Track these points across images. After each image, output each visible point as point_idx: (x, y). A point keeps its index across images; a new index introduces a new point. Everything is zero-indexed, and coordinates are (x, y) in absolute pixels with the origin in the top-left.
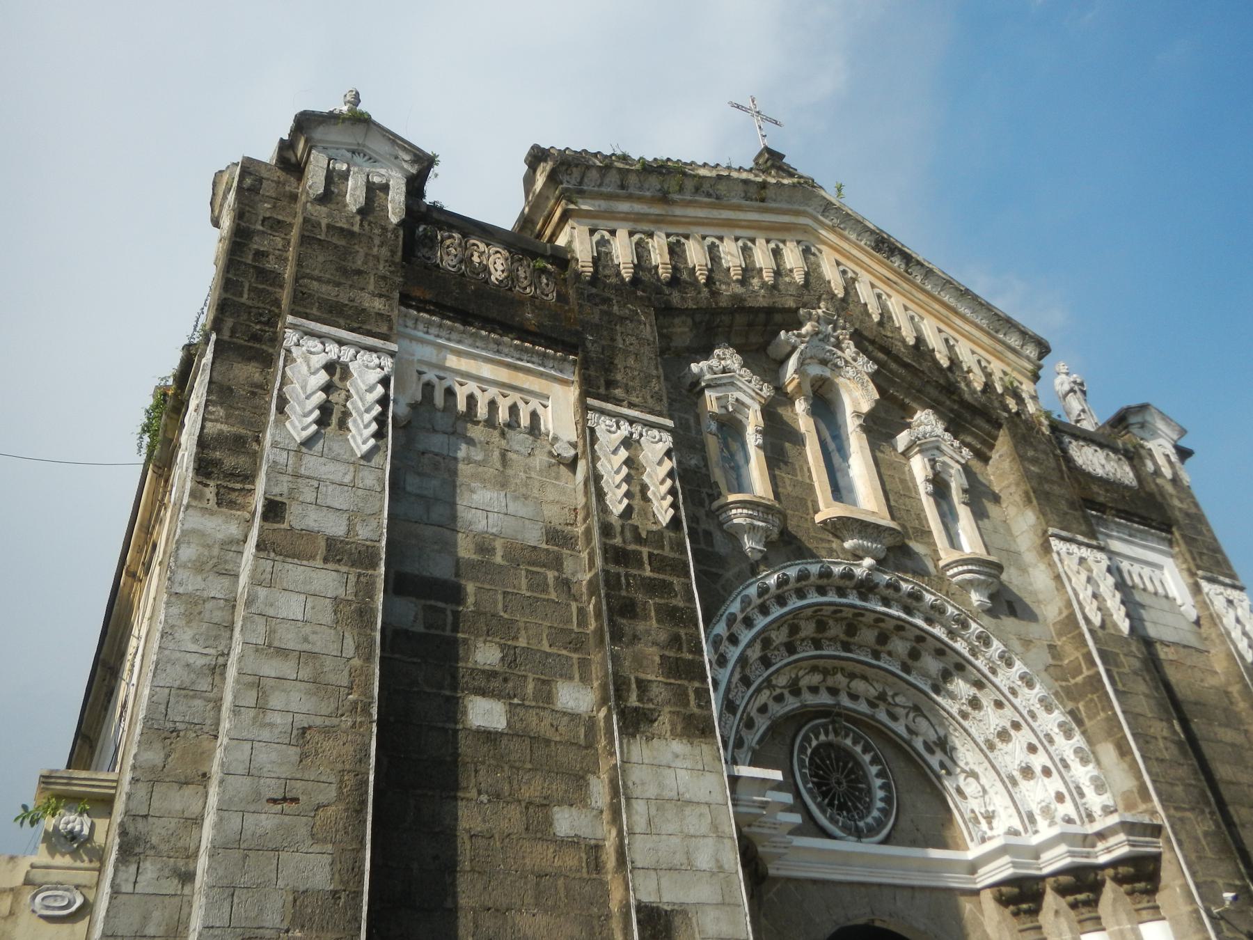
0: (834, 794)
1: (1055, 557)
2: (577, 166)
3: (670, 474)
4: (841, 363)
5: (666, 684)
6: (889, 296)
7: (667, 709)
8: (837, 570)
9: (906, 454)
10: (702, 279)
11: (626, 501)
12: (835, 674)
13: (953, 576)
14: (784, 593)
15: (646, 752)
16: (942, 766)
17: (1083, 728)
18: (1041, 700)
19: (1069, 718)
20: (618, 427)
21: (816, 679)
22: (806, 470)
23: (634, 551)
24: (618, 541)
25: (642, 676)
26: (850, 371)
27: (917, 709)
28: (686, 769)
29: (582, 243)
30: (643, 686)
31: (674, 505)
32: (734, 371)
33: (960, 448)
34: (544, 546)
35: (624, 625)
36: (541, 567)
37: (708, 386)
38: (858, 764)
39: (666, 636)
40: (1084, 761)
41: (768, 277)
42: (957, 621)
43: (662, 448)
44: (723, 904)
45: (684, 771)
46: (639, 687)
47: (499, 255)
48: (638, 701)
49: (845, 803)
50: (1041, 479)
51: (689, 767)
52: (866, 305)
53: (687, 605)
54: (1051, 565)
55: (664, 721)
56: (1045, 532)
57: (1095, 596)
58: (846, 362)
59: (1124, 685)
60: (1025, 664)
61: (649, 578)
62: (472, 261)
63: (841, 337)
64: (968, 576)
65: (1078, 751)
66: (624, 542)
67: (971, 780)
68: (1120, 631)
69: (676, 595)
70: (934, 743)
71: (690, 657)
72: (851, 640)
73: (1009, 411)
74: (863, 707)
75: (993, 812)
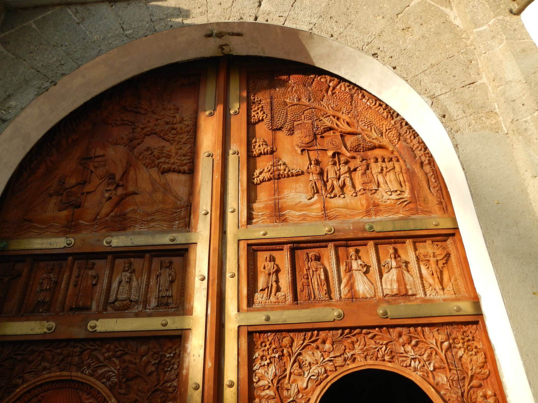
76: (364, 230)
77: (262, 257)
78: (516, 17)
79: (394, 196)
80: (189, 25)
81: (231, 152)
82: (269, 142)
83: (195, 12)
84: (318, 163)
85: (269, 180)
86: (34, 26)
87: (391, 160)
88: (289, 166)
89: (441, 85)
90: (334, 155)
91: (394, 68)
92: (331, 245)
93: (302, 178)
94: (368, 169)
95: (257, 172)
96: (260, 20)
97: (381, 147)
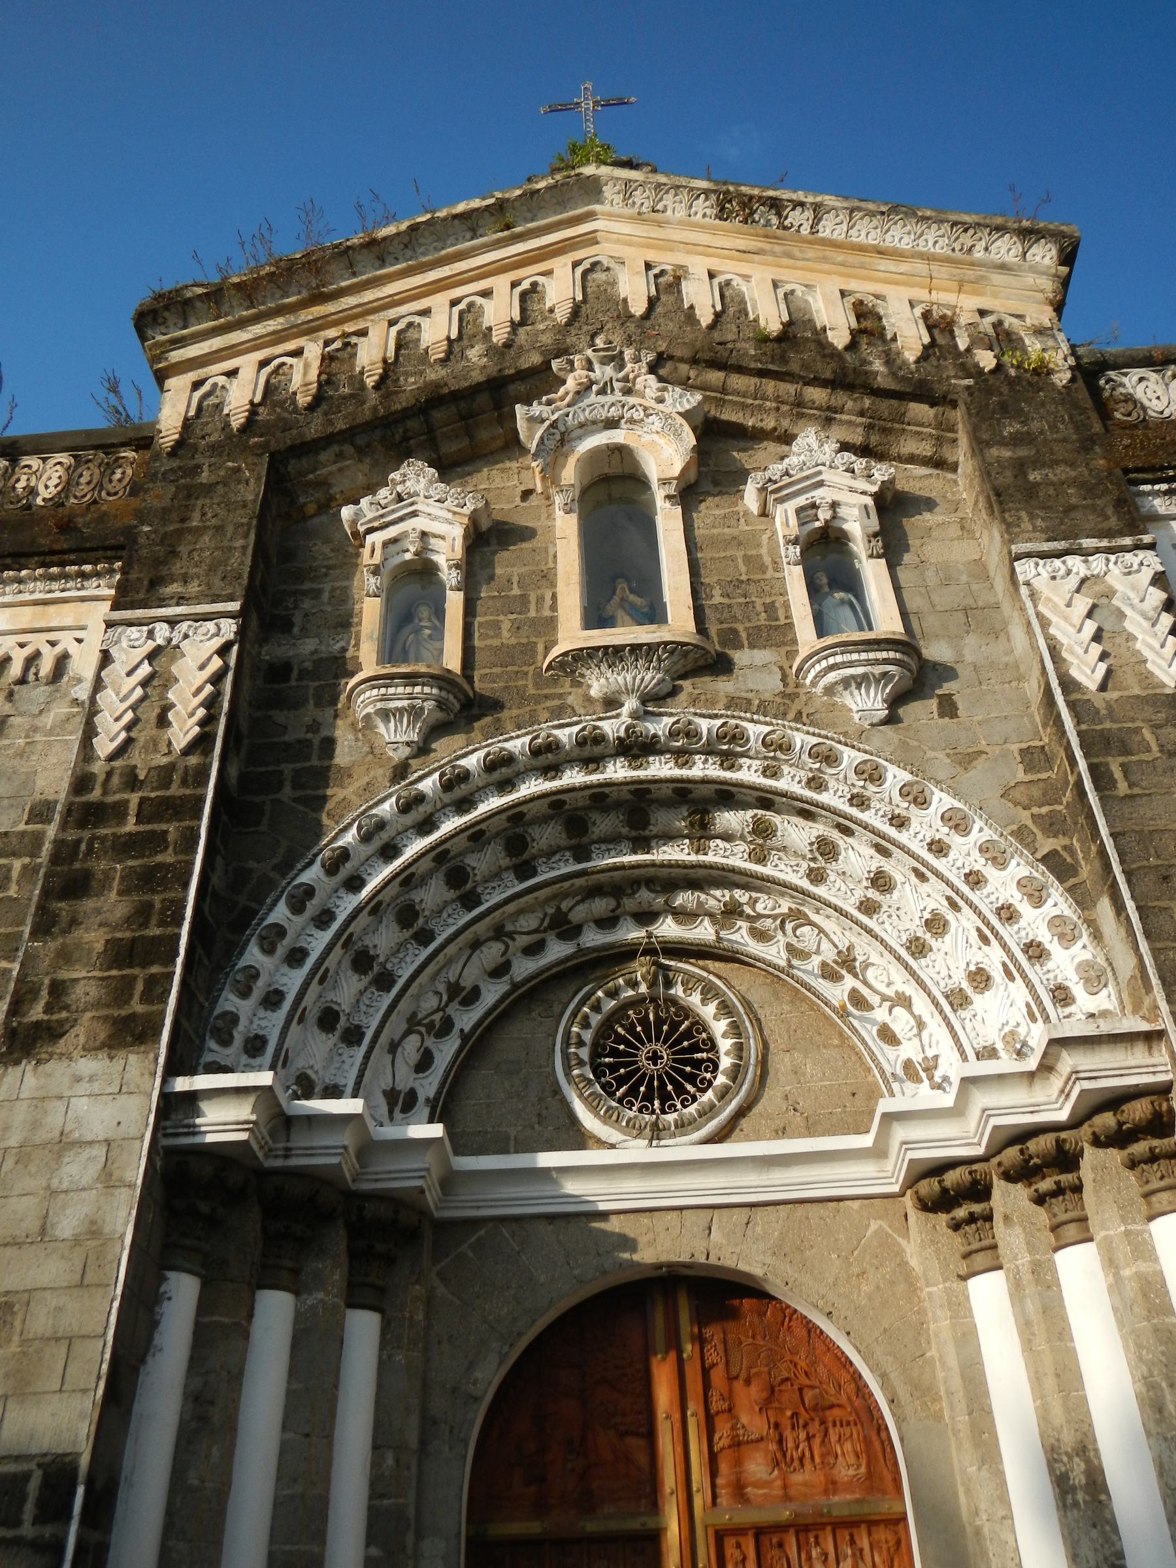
0: (644, 1074)
1: (1024, 590)
2: (166, 308)
3: (217, 679)
4: (638, 415)
5: (102, 979)
6: (746, 278)
7: (88, 1015)
8: (566, 735)
9: (764, 514)
10: (370, 382)
11: (123, 735)
12: (634, 893)
13: (814, 684)
14: (472, 794)
15: (31, 1081)
16: (854, 994)
17: (1072, 881)
18: (984, 849)
19: (1042, 867)
20: (151, 635)
21: (601, 906)
22: (548, 596)
23: (115, 803)
24: (96, 795)
25: (64, 975)
26: (655, 422)
27: (796, 915)
28: (90, 1096)
29: (174, 406)
30: (58, 989)
31: (208, 722)
32: (417, 494)
33: (867, 468)
34: (22, 827)
35: (60, 909)
36: (7, 856)
37: (370, 531)
38: (699, 1025)
39: (126, 910)
40: (1067, 938)
41: (499, 336)
42: (814, 753)
43: (217, 643)
44: (81, 1285)
45: (85, 1099)
46: (50, 994)
47: (58, 467)
48: (45, 1012)
49: (662, 1085)
50: (1021, 467)
51: (96, 1091)
52: (692, 307)
53: (181, 857)
54: (1022, 609)
55: (79, 1035)
56: (1010, 553)
57: (1097, 637)
58: (645, 409)
59: (1131, 786)
60: (956, 795)
61: (130, 834)
62: (14, 488)
63: (631, 376)
64: (832, 676)
65: (1056, 923)
66: (105, 793)
67: (898, 1011)
68: (1164, 685)
69: (166, 848)
70: (835, 962)
71: (158, 931)
72: (647, 833)
73: (978, 372)
74: (704, 932)
75: (936, 1057)
76: (822, 1515)
77: (730, 1542)
78: (963, 1283)
79: (851, 1472)
80: (638, 1264)
81: (689, 1413)
82: (726, 1395)
83: (642, 1241)
84: (777, 1426)
85: (730, 1447)
86: (470, 1254)
87: (848, 1424)
88: (749, 1429)
89: (891, 1359)
90: (792, 1417)
91: (848, 1334)
92: (792, 1531)
93: (762, 1445)
94: (826, 1435)
95: (717, 1437)
96: (713, 1260)
97: (839, 1406)
